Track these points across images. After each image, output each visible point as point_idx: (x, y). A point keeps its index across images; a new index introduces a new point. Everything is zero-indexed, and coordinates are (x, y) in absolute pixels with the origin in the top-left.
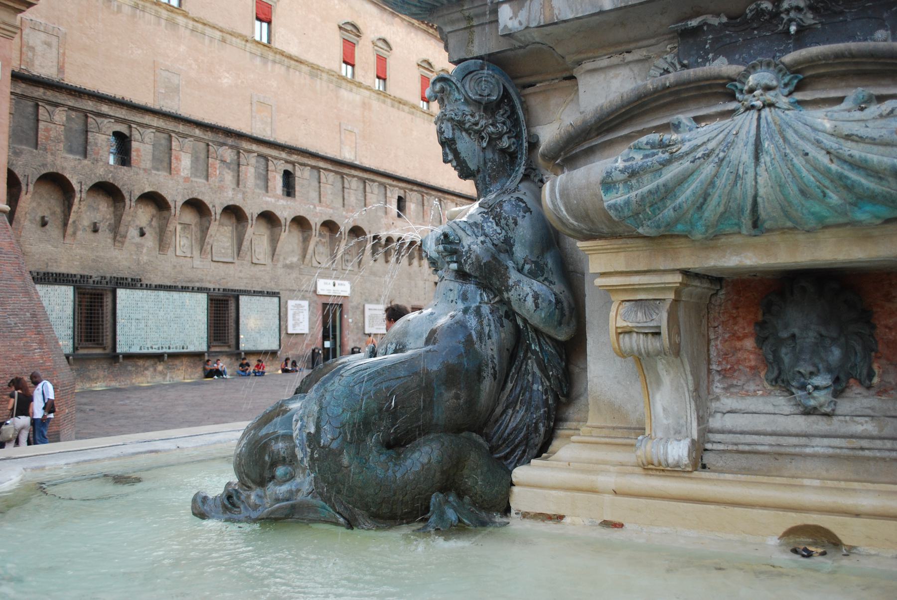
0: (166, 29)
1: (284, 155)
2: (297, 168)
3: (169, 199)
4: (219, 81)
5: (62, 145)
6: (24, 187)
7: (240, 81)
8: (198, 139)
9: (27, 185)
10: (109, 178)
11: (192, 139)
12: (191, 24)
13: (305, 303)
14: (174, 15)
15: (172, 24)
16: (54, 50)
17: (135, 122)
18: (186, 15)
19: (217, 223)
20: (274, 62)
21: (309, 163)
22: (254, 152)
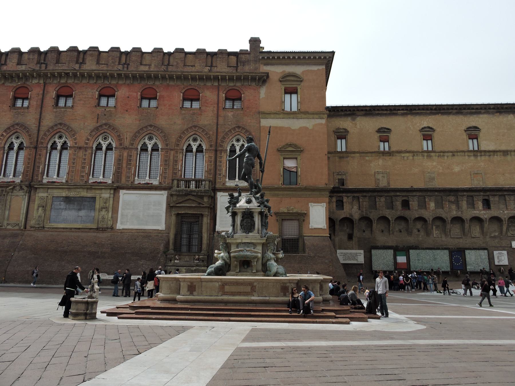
0: (427, 159)
1: (482, 194)
2: (490, 197)
3: (427, 218)
4: (453, 170)
5: (384, 207)
6: (373, 222)
7: (464, 168)
8: (437, 196)
9: (374, 221)
10: (402, 215)
11: (434, 196)
12: (437, 154)
13: (505, 252)
14: (429, 154)
15: (429, 157)
16: (386, 178)
17: (410, 196)
18: (435, 152)
19: (449, 224)
20: (481, 156)
21: (498, 194)
22: (465, 195)
